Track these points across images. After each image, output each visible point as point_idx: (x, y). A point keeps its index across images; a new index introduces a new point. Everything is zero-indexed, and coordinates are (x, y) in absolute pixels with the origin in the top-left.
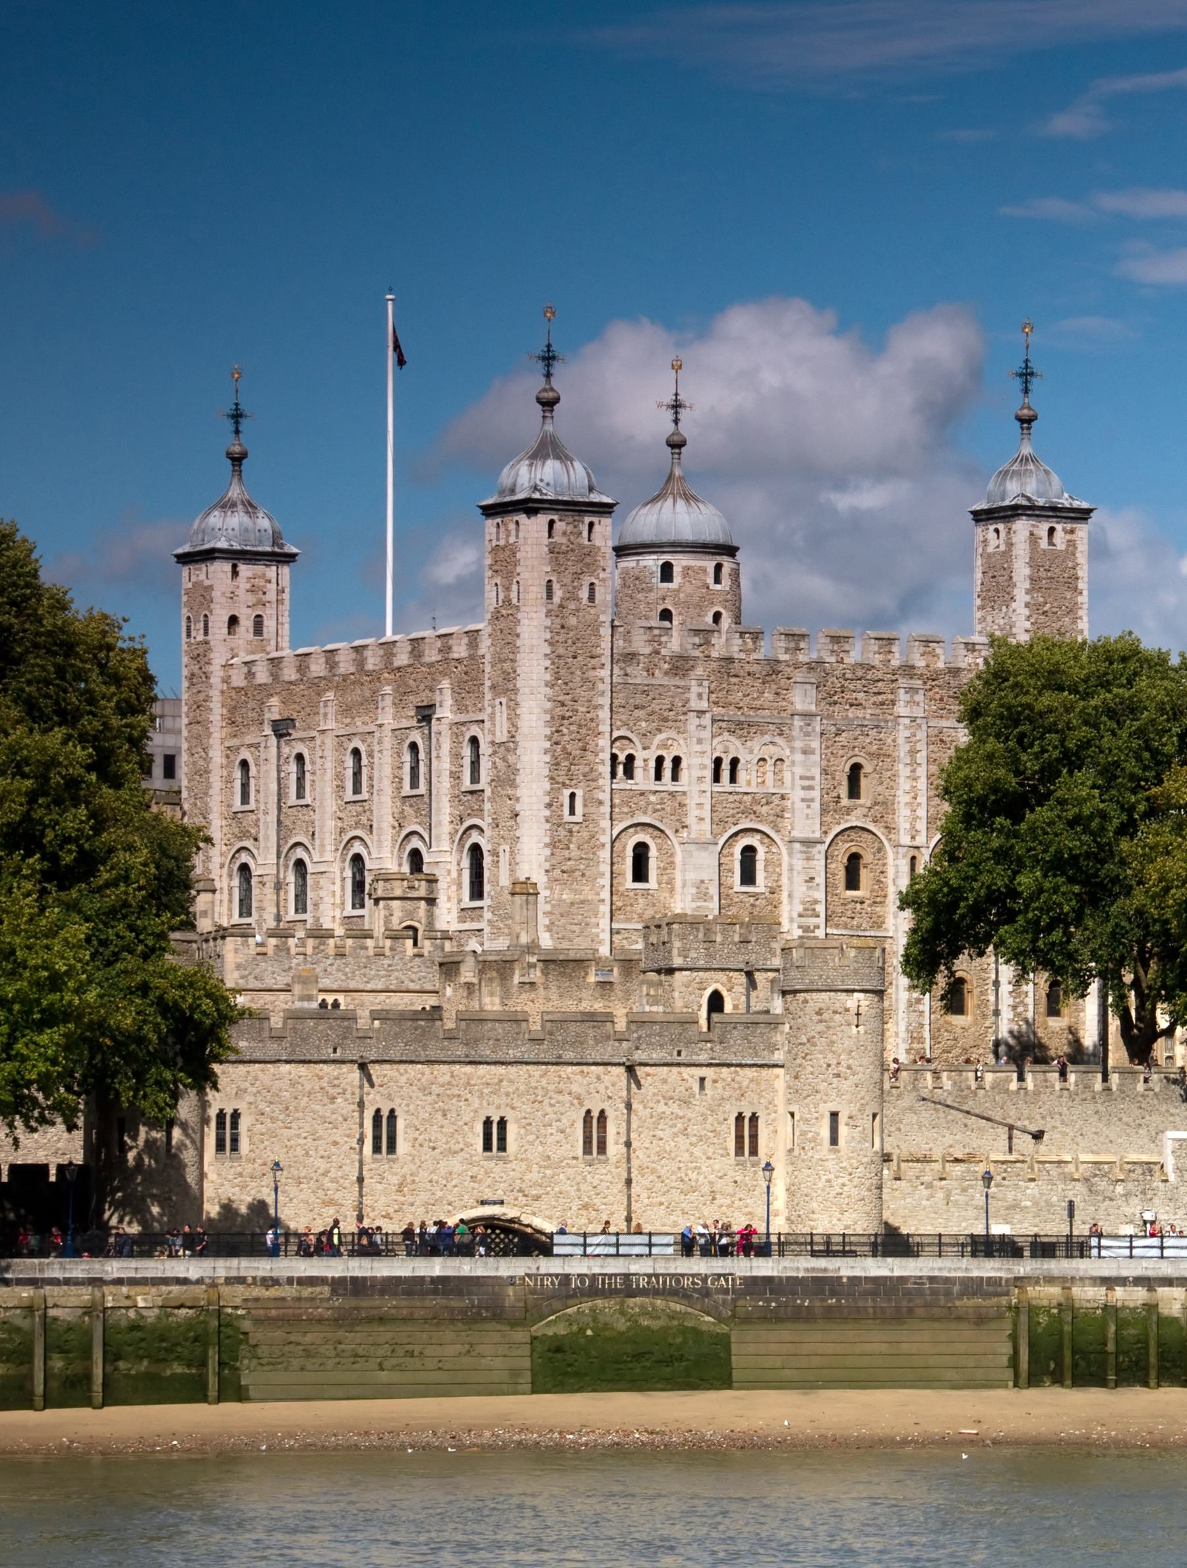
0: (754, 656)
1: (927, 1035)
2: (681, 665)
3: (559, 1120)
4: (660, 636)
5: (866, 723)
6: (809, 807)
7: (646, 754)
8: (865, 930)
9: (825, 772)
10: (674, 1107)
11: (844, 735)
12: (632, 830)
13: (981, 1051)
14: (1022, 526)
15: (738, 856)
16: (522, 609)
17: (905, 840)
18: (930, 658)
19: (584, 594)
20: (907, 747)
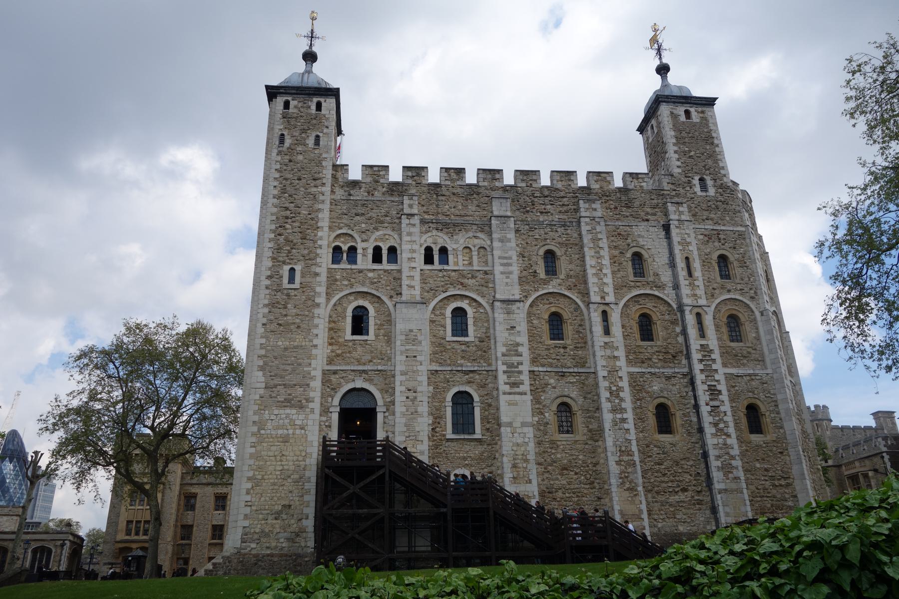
0: (459, 183)
1: (634, 448)
2: (395, 188)
4: (379, 171)
5: (554, 223)
6: (508, 277)
7: (364, 245)
8: (570, 367)
9: (522, 255)
11: (537, 231)
12: (352, 298)
13: (691, 463)
14: (664, 110)
17: (595, 298)
18: (605, 184)
19: (311, 142)
20: (590, 236)
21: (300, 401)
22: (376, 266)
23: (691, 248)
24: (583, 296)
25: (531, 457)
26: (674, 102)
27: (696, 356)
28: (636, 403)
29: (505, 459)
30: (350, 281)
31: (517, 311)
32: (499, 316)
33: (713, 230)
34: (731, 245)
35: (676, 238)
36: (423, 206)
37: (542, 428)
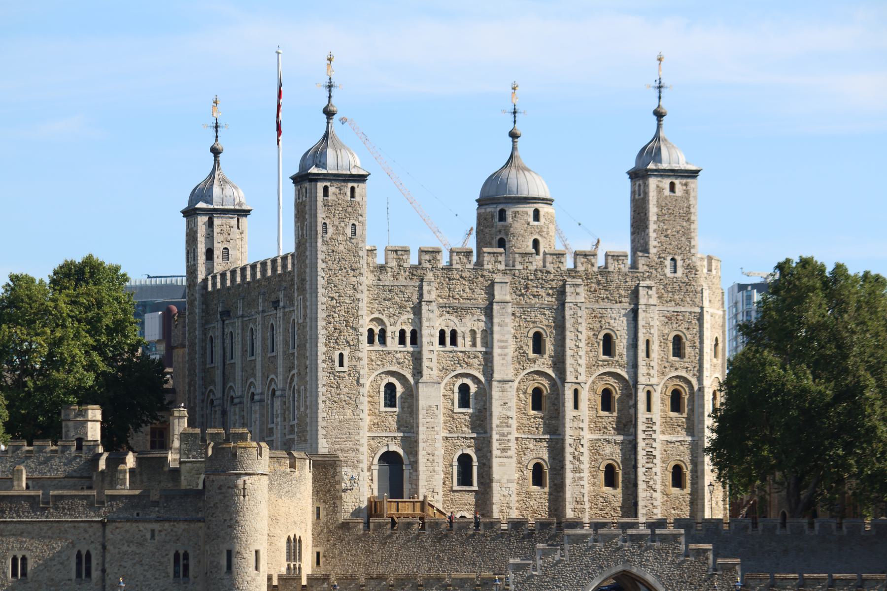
0: (468, 266)
1: (586, 499)
3: (59, 557)
4: (402, 255)
5: (543, 306)
6: (503, 359)
10: (133, 548)
14: (653, 182)
15: (456, 390)
16: (308, 241)
17: (570, 378)
19: (349, 231)
20: (572, 320)
21: (353, 462)
22: (401, 348)
23: (652, 331)
24: (561, 373)
25: (514, 505)
26: (661, 176)
27: (641, 427)
28: (591, 464)
29: (494, 507)
30: (381, 361)
31: (509, 390)
32: (496, 393)
33: (674, 312)
34: (686, 325)
35: (641, 322)
36: (437, 289)
37: (520, 482)
